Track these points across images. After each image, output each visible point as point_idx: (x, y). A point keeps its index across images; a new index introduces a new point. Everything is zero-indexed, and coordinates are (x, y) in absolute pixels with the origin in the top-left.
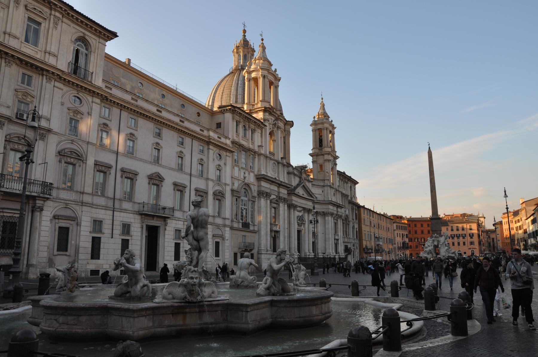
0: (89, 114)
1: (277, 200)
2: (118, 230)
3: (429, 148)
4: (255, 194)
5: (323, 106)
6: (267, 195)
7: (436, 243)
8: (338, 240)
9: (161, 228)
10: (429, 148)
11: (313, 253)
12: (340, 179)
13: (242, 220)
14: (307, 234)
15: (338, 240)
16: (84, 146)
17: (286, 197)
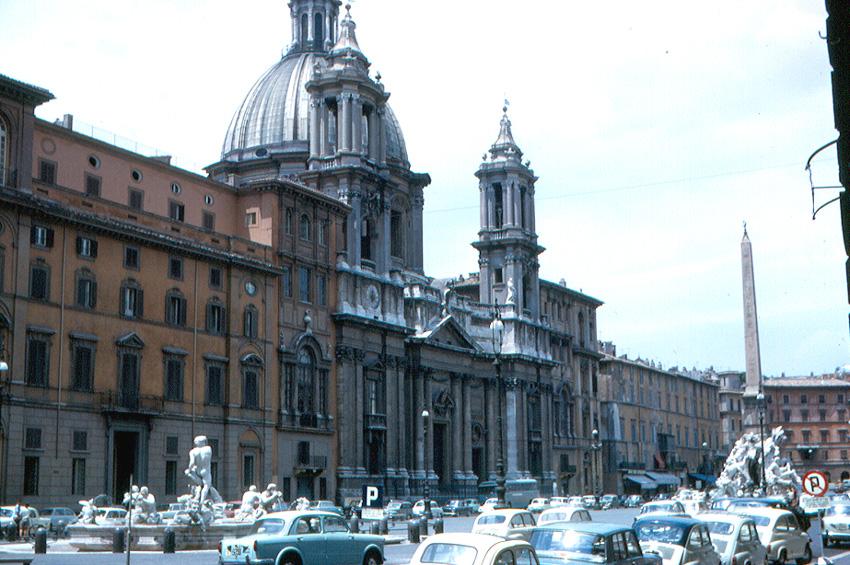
0: (15, 246)
1: (378, 366)
2: (67, 441)
3: (746, 233)
4: (330, 356)
5: (507, 128)
6: (358, 355)
7: (752, 454)
8: (538, 444)
9: (141, 434)
10: (746, 233)
11: (475, 473)
12: (549, 298)
13: (301, 409)
14: (458, 433)
15: (538, 444)
16: (9, 303)
17: (401, 354)
